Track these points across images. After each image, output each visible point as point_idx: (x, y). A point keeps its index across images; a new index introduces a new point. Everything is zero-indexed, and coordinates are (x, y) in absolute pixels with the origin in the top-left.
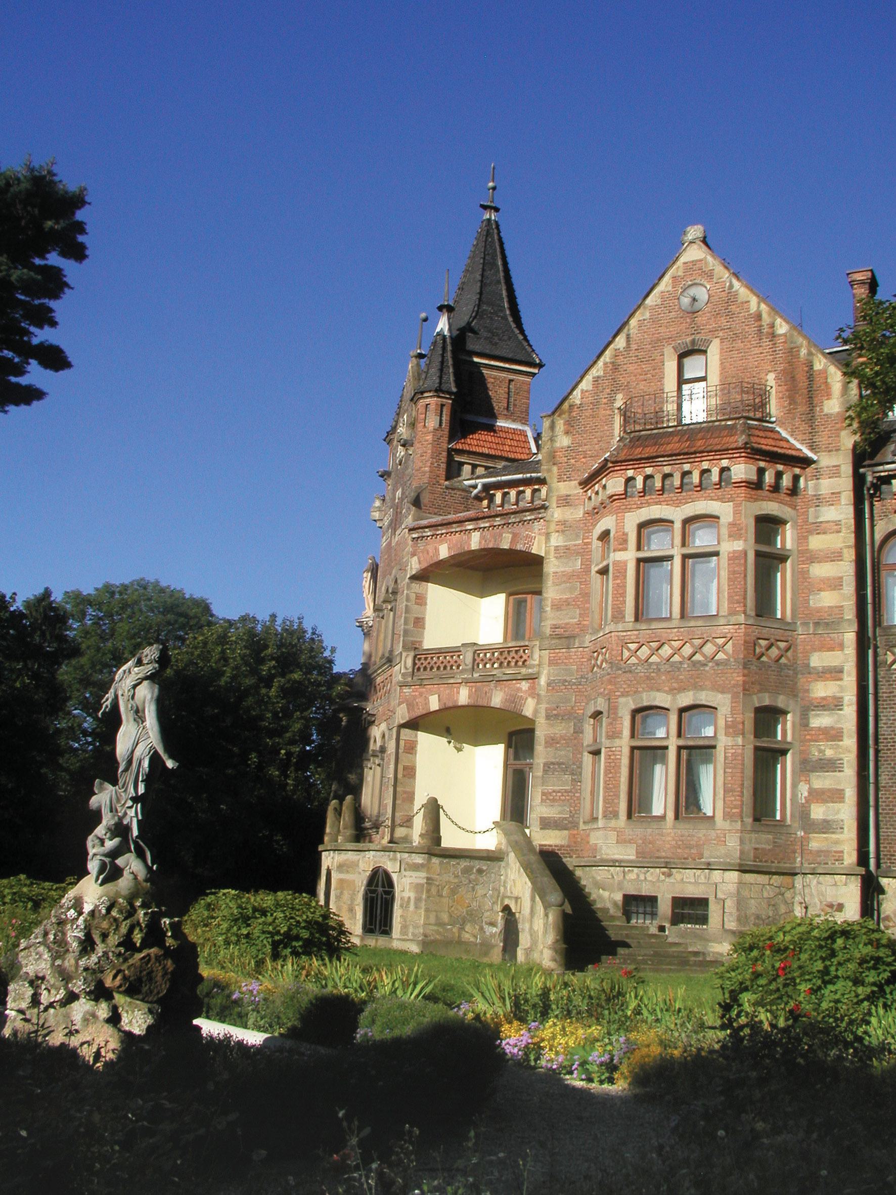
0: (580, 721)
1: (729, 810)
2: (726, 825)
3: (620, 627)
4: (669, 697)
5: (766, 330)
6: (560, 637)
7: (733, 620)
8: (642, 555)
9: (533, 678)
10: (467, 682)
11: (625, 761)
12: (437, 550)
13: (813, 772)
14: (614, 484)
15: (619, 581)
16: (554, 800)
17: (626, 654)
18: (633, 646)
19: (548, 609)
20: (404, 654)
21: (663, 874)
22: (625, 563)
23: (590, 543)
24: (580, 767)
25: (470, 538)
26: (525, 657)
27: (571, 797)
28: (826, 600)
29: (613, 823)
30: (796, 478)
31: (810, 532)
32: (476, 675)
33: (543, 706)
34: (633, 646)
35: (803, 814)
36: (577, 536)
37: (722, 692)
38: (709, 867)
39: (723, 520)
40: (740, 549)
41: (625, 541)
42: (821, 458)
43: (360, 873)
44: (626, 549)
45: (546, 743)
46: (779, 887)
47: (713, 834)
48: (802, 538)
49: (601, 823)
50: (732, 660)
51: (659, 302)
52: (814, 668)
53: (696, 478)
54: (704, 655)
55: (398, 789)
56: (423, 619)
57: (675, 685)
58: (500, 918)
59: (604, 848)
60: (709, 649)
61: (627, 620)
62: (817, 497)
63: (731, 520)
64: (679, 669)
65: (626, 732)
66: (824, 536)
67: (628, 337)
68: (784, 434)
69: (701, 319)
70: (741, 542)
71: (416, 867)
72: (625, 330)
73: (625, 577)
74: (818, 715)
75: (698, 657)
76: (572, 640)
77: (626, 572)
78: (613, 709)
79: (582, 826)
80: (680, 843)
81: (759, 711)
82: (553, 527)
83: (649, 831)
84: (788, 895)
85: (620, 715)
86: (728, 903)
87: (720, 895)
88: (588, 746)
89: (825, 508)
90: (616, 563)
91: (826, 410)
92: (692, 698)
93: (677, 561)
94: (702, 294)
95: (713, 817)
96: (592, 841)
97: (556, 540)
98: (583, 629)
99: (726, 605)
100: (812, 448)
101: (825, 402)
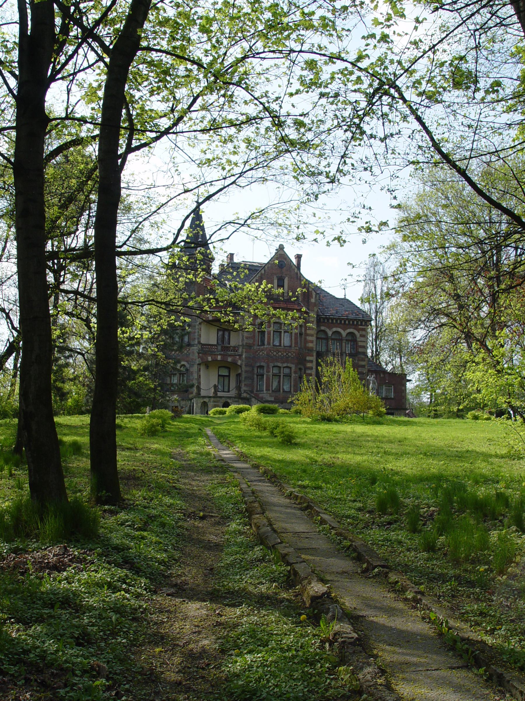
9: (240, 356)
10: (220, 354)
28: (310, 345)
33: (244, 363)
48: (305, 330)
60: (290, 354)
98: (254, 345)
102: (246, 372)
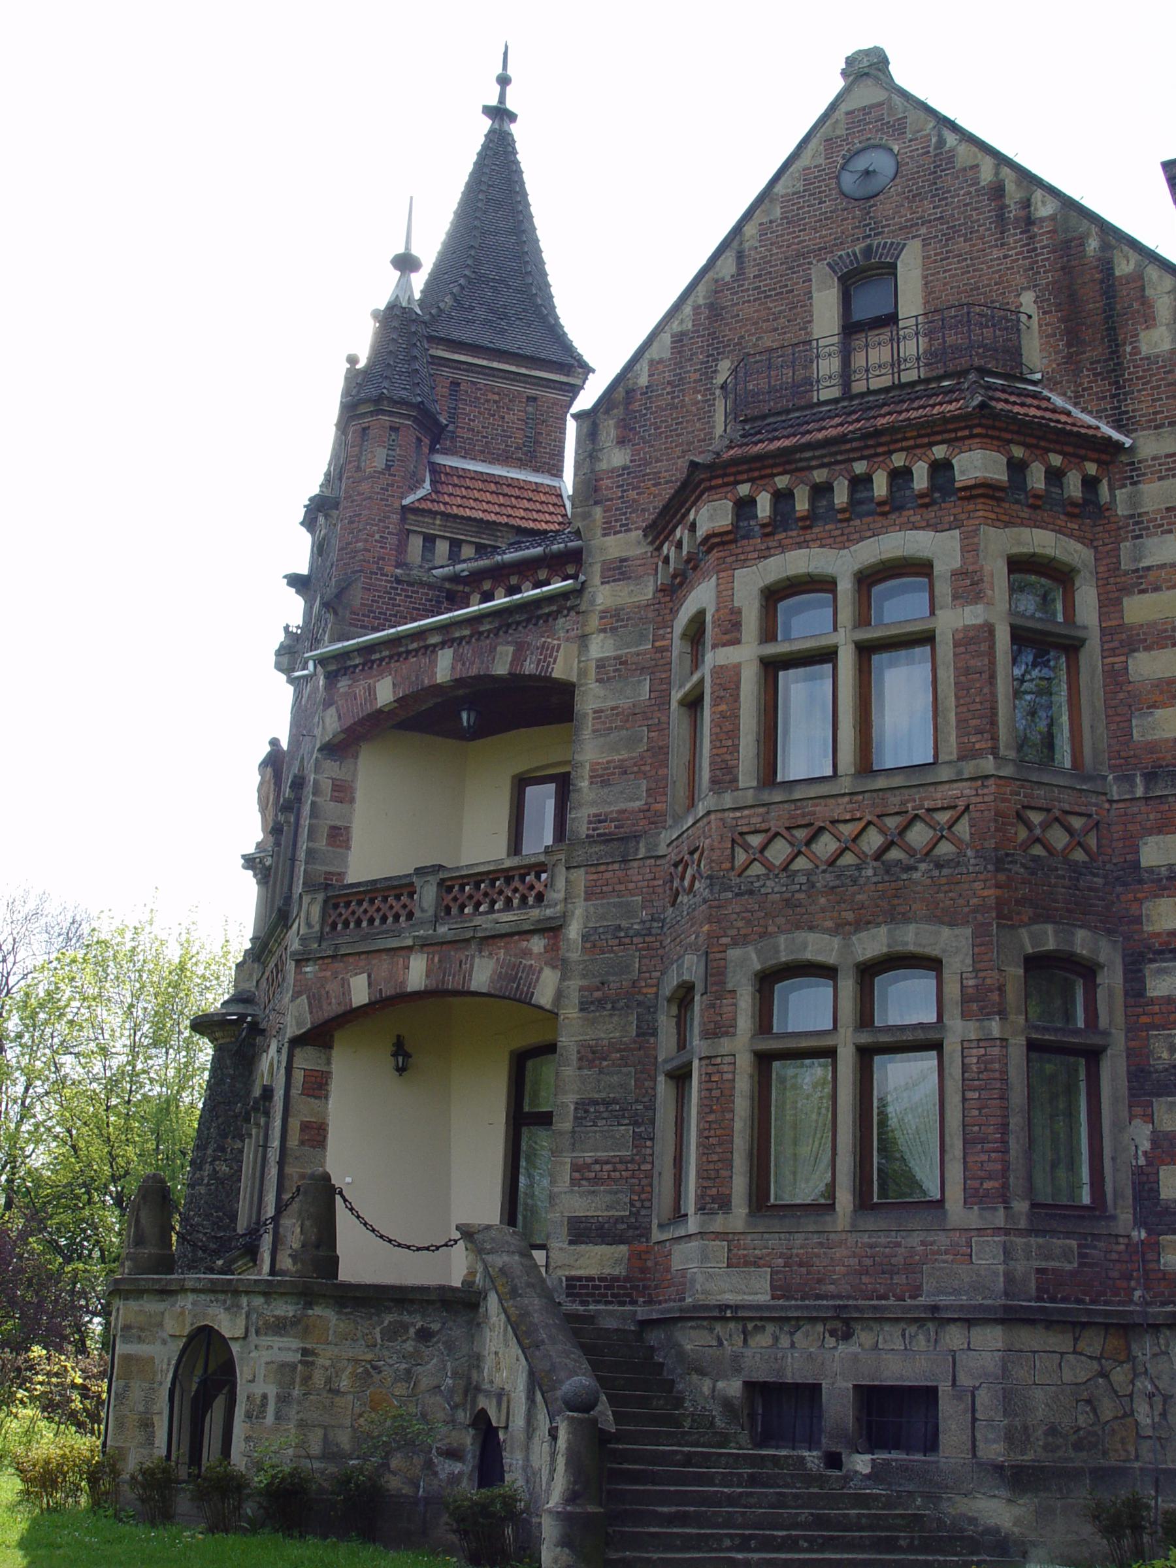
0: (651, 1009)
1: (976, 1184)
2: (973, 1218)
3: (728, 800)
4: (836, 942)
5: (1013, 212)
6: (606, 839)
7: (969, 769)
8: (771, 649)
9: (552, 929)
10: (424, 945)
11: (743, 1085)
12: (371, 691)
13: (1159, 1095)
14: (713, 515)
15: (723, 707)
16: (596, 1181)
17: (741, 857)
18: (755, 841)
19: (584, 784)
20: (306, 899)
21: (833, 1333)
22: (737, 667)
23: (667, 649)
24: (651, 1107)
25: (433, 663)
26: (539, 887)
27: (635, 1175)
29: (718, 1223)
30: (1090, 484)
31: (1126, 590)
32: (442, 930)
33: (575, 984)
34: (755, 841)
35: (1145, 1187)
36: (642, 637)
37: (952, 924)
38: (936, 1317)
39: (939, 568)
40: (980, 621)
41: (737, 625)
42: (1141, 442)
43: (164, 1342)
44: (737, 642)
45: (580, 1059)
46: (1098, 1359)
47: (942, 1240)
48: (1110, 603)
49: (693, 1225)
50: (969, 853)
51: (800, 186)
52: (1150, 870)
53: (880, 486)
54: (910, 851)
55: (288, 1170)
56: (347, 828)
57: (850, 916)
58: (468, 1440)
59: (700, 1278)
60: (919, 835)
61: (741, 785)
62: (1136, 518)
63: (957, 564)
64: (855, 881)
65: (745, 1023)
66: (1155, 595)
67: (740, 256)
68: (1058, 401)
69: (883, 209)
70: (980, 608)
71: (279, 1327)
72: (735, 244)
73: (736, 698)
74: (1160, 971)
75: (895, 854)
76: (632, 844)
77: (738, 687)
78: (716, 974)
79: (657, 1235)
80: (868, 1262)
81: (1036, 963)
82: (594, 622)
83: (799, 1240)
84: (1119, 1375)
85: (730, 986)
86: (983, 1397)
87: (964, 1380)
88: (665, 1061)
89: (1155, 539)
90: (718, 671)
91: (1145, 350)
92: (885, 941)
93: (846, 658)
94: (883, 163)
95: (941, 1203)
96: (676, 1264)
97: (600, 647)
98: (656, 820)
99: (953, 739)
100: (1119, 427)
101: (1142, 335)
102: (591, 1056)
